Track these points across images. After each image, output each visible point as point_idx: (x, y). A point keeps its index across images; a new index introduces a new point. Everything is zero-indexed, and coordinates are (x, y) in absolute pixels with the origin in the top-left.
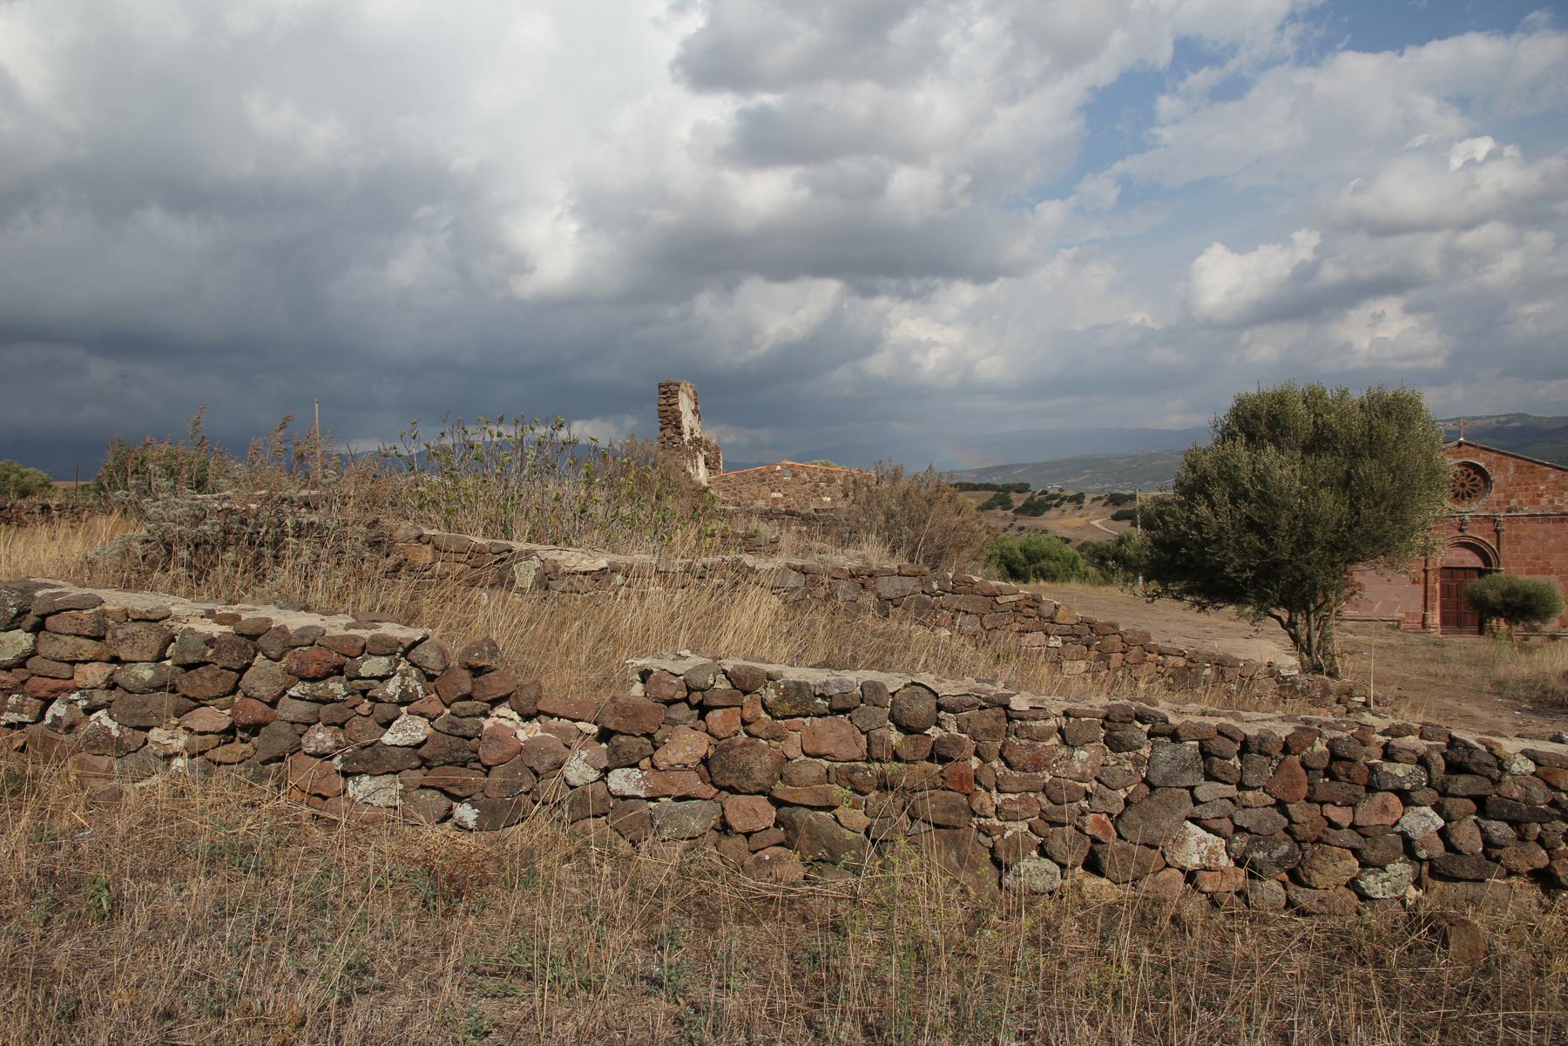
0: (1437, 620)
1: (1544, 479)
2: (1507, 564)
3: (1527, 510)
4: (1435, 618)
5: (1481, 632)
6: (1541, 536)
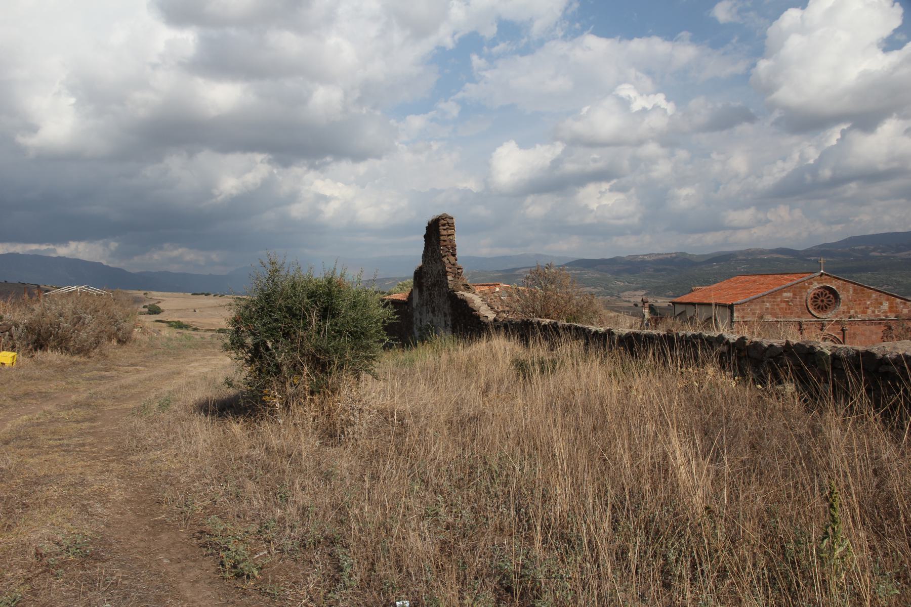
1: (869, 297)
3: (860, 317)
6: (868, 333)
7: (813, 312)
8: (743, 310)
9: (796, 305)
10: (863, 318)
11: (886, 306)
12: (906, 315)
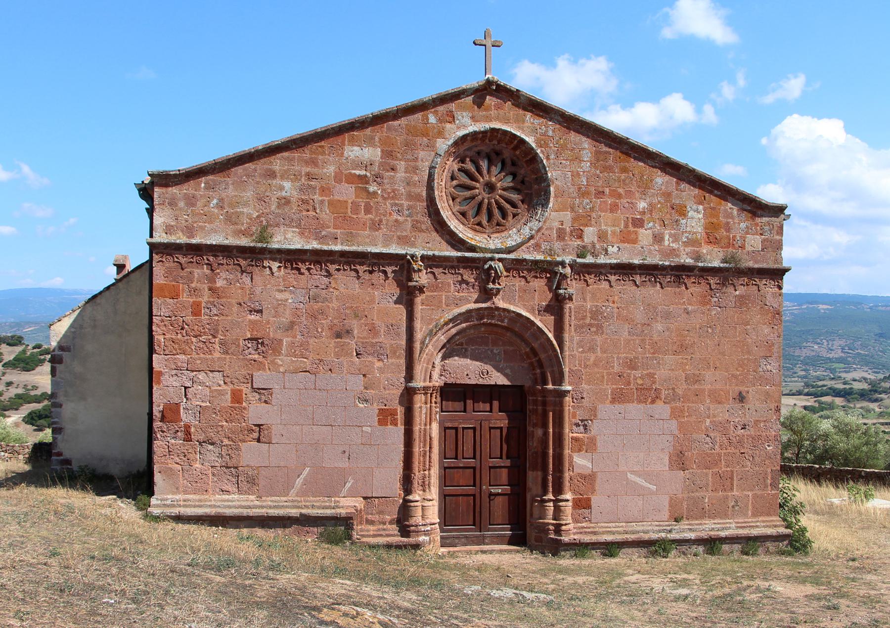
0: (433, 514)
1: (645, 187)
2: (577, 378)
3: (615, 255)
4: (428, 506)
5: (519, 540)
6: (639, 315)
7: (454, 224)
8: (191, 201)
9: (394, 195)
10: (625, 259)
11: (695, 219)
12: (753, 254)
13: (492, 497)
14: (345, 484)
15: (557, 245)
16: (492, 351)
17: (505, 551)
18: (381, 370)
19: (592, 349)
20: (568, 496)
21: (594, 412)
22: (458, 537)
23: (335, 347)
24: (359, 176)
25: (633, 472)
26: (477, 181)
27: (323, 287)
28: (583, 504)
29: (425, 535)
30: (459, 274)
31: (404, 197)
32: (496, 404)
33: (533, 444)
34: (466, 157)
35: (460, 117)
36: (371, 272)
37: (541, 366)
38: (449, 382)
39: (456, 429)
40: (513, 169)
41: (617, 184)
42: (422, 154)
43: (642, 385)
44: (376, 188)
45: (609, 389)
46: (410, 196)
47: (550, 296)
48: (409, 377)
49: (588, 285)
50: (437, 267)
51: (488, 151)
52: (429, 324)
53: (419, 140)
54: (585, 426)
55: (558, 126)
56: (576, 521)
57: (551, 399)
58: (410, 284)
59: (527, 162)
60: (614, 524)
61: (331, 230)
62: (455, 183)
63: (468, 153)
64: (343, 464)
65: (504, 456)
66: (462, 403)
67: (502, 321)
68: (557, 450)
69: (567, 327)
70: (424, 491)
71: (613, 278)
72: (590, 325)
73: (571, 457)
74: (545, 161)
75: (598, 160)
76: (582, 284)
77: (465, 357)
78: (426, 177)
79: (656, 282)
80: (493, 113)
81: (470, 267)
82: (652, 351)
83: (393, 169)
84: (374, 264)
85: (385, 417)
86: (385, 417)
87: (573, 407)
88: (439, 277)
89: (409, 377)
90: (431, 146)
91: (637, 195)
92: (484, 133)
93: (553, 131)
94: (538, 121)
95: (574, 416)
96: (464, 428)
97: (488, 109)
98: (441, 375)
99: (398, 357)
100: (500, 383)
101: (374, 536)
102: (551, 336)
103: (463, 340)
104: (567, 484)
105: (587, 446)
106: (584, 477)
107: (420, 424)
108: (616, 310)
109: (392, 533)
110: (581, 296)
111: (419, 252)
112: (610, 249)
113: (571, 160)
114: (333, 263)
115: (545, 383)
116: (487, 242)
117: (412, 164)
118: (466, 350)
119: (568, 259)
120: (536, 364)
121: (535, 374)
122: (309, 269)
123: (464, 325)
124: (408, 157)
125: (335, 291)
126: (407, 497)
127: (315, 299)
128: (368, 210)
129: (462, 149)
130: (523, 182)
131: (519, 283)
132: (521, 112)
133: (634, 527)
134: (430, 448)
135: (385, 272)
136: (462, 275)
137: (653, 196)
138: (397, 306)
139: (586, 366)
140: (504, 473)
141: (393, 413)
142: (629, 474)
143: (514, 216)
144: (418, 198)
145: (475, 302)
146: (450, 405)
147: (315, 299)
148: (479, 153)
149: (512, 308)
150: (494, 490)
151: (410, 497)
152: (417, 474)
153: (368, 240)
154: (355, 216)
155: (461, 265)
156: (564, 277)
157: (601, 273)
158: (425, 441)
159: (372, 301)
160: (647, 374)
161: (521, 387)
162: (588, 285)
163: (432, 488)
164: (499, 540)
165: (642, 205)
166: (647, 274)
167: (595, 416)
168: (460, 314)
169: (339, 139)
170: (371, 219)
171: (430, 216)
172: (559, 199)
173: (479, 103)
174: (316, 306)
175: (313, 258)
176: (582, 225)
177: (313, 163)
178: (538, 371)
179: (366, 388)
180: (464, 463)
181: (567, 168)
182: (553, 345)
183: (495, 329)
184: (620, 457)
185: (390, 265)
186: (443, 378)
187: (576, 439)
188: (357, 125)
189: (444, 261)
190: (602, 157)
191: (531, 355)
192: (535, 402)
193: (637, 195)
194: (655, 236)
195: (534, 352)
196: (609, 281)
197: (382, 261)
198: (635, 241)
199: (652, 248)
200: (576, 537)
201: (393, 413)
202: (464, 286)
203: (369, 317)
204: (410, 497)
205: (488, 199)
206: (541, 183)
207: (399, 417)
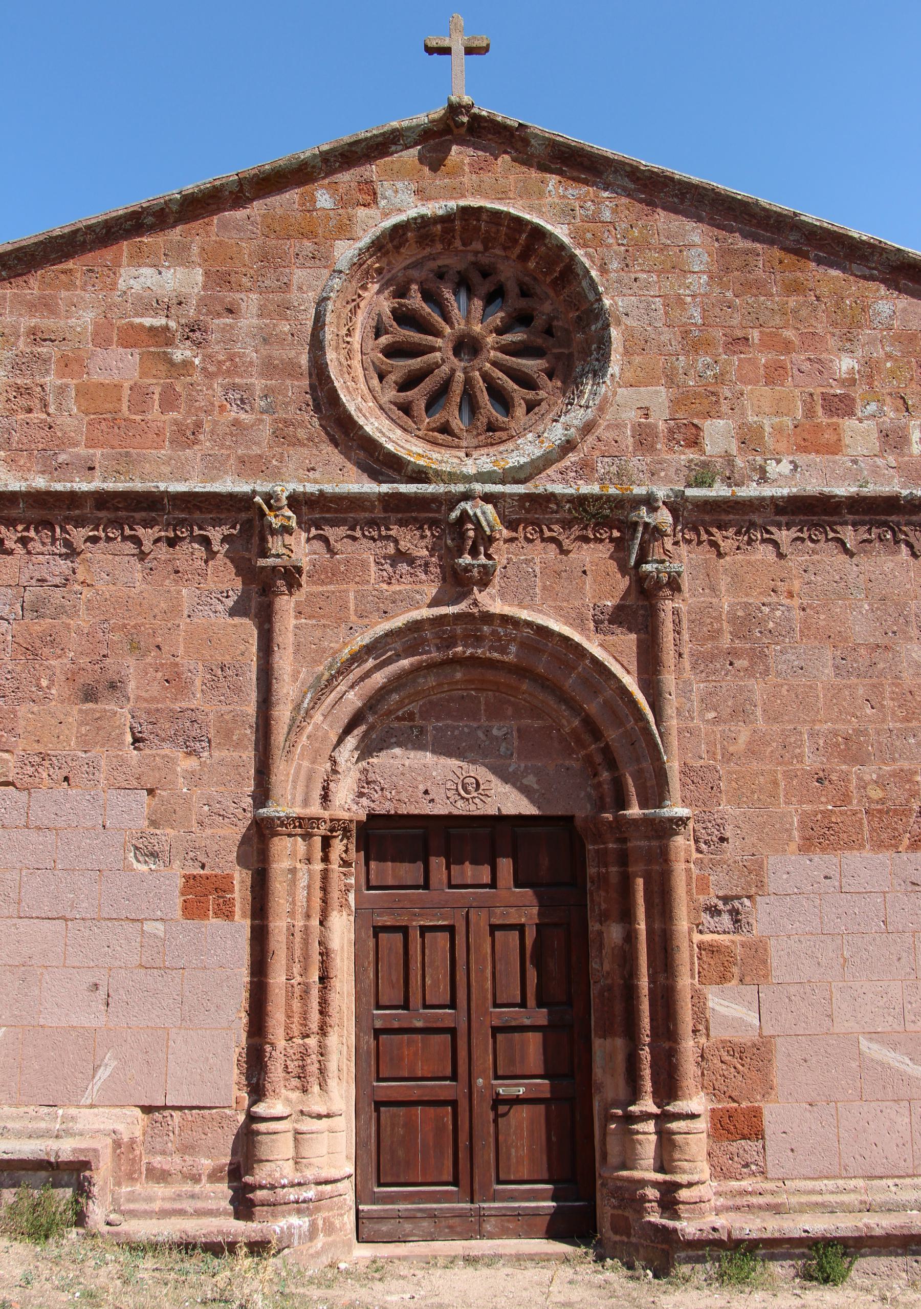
1: (849, 331)
4: (321, 1135)
6: (860, 624)
7: (377, 426)
13: (502, 1109)
14: (95, 1070)
15: (636, 463)
16: (487, 732)
17: (531, 1257)
18: (194, 778)
19: (740, 713)
20: (695, 1102)
21: (755, 875)
22: (410, 1217)
23: (82, 723)
24: (152, 329)
25: (873, 1035)
26: (438, 334)
27: (57, 580)
28: (738, 1126)
29: (299, 1212)
30: (388, 538)
31: (254, 370)
32: (505, 865)
33: (602, 966)
34: (409, 282)
35: (389, 193)
36: (172, 543)
37: (612, 763)
38: (380, 810)
39: (404, 930)
40: (522, 303)
41: (778, 320)
42: (299, 275)
43: (882, 801)
44: (188, 353)
45: (792, 813)
46: (269, 368)
47: (624, 583)
48: (262, 794)
49: (720, 555)
50: (334, 523)
51: (461, 266)
52: (316, 662)
53: (292, 246)
54: (735, 914)
55: (624, 200)
56: (721, 1173)
57: (637, 843)
58: (262, 562)
59: (554, 283)
60: (830, 1184)
61: (81, 450)
62: (384, 340)
63: (414, 273)
64: (91, 1016)
65: (531, 1001)
66: (420, 865)
67: (503, 650)
68: (661, 979)
69: (669, 656)
70: (305, 1091)
71: (784, 536)
72: (732, 653)
73: (698, 998)
74: (594, 273)
75: (727, 270)
76: (705, 553)
77: (421, 747)
78: (310, 324)
79: (897, 542)
80: (468, 179)
81: (415, 520)
82: (900, 714)
83: (230, 311)
84: (177, 524)
85: (203, 896)
86: (203, 896)
87: (699, 863)
88: (338, 546)
89: (262, 794)
90: (321, 258)
91: (832, 342)
92: (447, 219)
93: (615, 211)
94: (574, 191)
95: (703, 885)
96: (424, 930)
97: (456, 172)
98: (361, 795)
99: (238, 745)
100: (510, 809)
101: (164, 1214)
102: (630, 682)
103: (414, 707)
104: (690, 1068)
105: (741, 966)
106: (738, 1051)
107: (292, 914)
108: (797, 614)
109: (211, 1205)
110: (706, 583)
111: (285, 488)
112: (772, 468)
113: (659, 273)
114: (79, 523)
115: (622, 803)
116: (461, 464)
117: (277, 297)
118: (422, 731)
119: (661, 492)
120: (598, 759)
121: (599, 784)
122: (24, 541)
123: (405, 663)
124: (268, 283)
125: (85, 590)
126: (254, 1109)
127: (37, 609)
128: (169, 401)
129: (400, 263)
130: (549, 331)
131: (542, 555)
132: (534, 174)
133: (886, 1191)
134: (324, 979)
135: (206, 541)
136: (396, 542)
137: (871, 342)
138: (237, 620)
139: (728, 757)
140: (534, 1041)
141: (222, 886)
142: (864, 1043)
143: (531, 406)
144: (289, 369)
145: (430, 606)
146: (389, 871)
147: (37, 609)
148: (441, 275)
149: (525, 615)
150: (504, 1089)
151: (261, 1109)
152: (281, 1043)
153: (166, 469)
154: (138, 418)
155: (393, 517)
156: (655, 532)
157: (752, 525)
158: (306, 957)
159: (174, 610)
160: (894, 774)
161: (569, 819)
162: (720, 555)
163: (332, 1083)
164: (520, 1224)
165: (846, 364)
166: (872, 524)
167: (761, 885)
168: (389, 634)
169: (108, 254)
170: (176, 422)
171: (317, 409)
172: (637, 359)
173: (435, 161)
174: (40, 626)
175: (32, 514)
176: (697, 415)
177: (47, 306)
178: (605, 775)
179: (154, 823)
180: (426, 1018)
181: (651, 285)
182: (633, 703)
183: (490, 675)
184: (836, 995)
185: (217, 523)
186: (364, 801)
187: (712, 949)
188: (150, 220)
189: (349, 509)
190: (737, 263)
191: (587, 737)
192: (602, 858)
193: (832, 342)
194: (885, 435)
195: (591, 728)
196: (776, 544)
197: (197, 515)
198: (834, 448)
199: (880, 462)
200: (721, 1221)
201: (222, 886)
202: (404, 567)
203: (165, 648)
204: (261, 1109)
205: (465, 371)
206: (588, 325)
207: (237, 895)
